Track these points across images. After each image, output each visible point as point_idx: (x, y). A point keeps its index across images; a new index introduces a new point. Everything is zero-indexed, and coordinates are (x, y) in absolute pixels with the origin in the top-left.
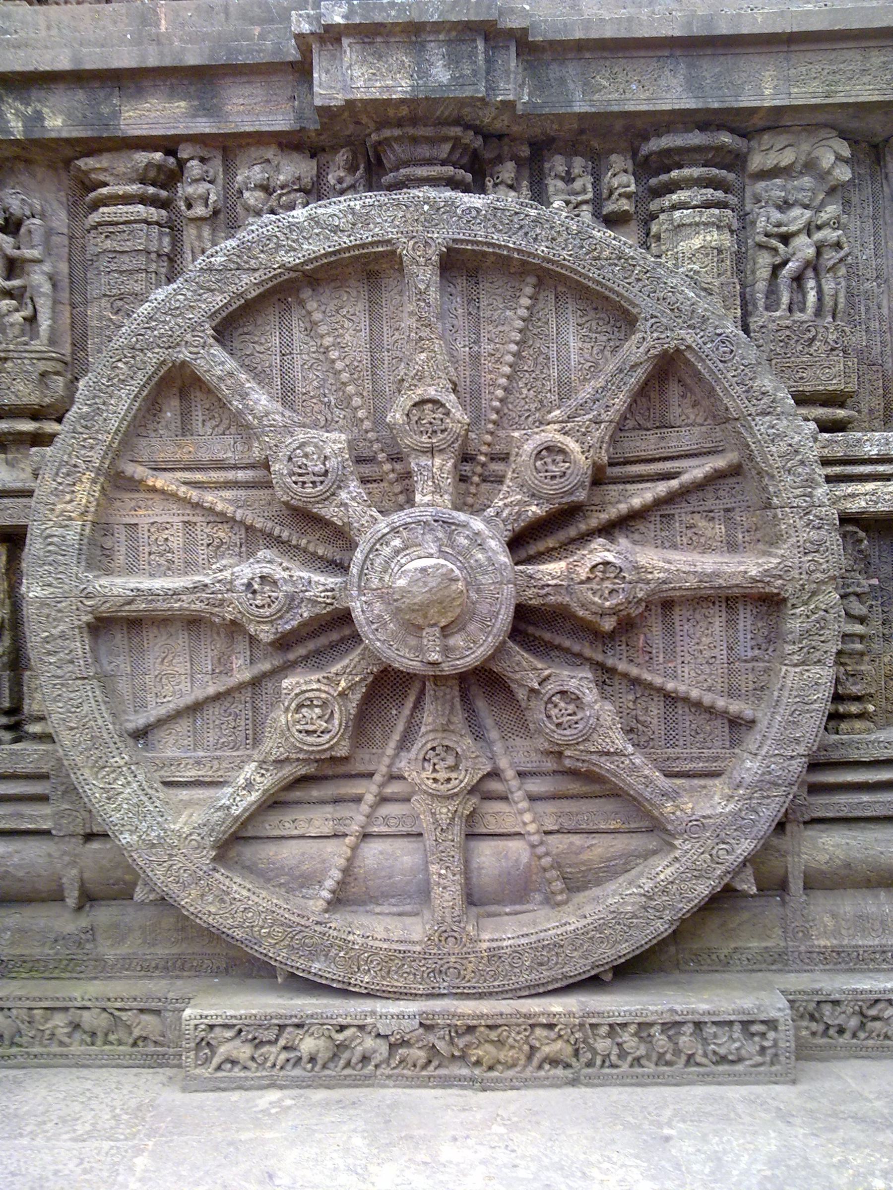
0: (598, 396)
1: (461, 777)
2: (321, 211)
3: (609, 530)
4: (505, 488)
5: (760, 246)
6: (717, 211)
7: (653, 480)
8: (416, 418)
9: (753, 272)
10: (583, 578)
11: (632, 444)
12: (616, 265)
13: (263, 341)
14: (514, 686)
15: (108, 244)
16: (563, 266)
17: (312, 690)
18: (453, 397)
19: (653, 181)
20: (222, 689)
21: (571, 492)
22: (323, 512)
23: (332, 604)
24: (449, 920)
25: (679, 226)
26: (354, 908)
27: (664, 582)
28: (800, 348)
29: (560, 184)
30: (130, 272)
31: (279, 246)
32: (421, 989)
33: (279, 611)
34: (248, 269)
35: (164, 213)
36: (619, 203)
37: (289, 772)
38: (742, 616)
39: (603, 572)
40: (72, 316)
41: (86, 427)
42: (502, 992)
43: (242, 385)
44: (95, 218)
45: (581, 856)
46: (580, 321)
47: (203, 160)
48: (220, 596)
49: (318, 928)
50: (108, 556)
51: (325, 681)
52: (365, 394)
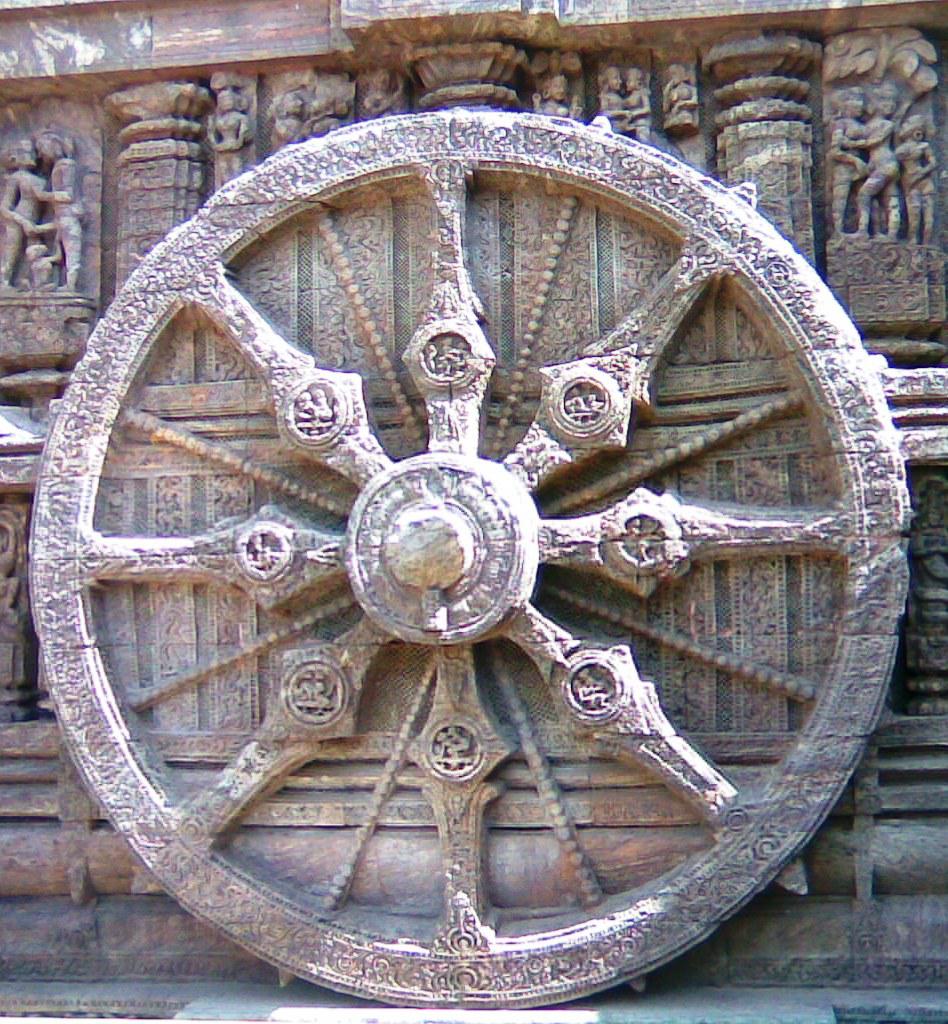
1: (476, 762)
5: (838, 161)
6: (785, 124)
7: (707, 423)
9: (831, 189)
13: (281, 276)
14: (536, 659)
15: (137, 182)
16: (599, 187)
17: (314, 662)
25: (744, 140)
27: (710, 539)
28: (880, 273)
29: (615, 98)
35: (196, 146)
36: (680, 116)
40: (103, 257)
44: (125, 155)
45: (616, 853)
47: (236, 89)
50: (117, 514)
51: (327, 652)
52: (387, 329)
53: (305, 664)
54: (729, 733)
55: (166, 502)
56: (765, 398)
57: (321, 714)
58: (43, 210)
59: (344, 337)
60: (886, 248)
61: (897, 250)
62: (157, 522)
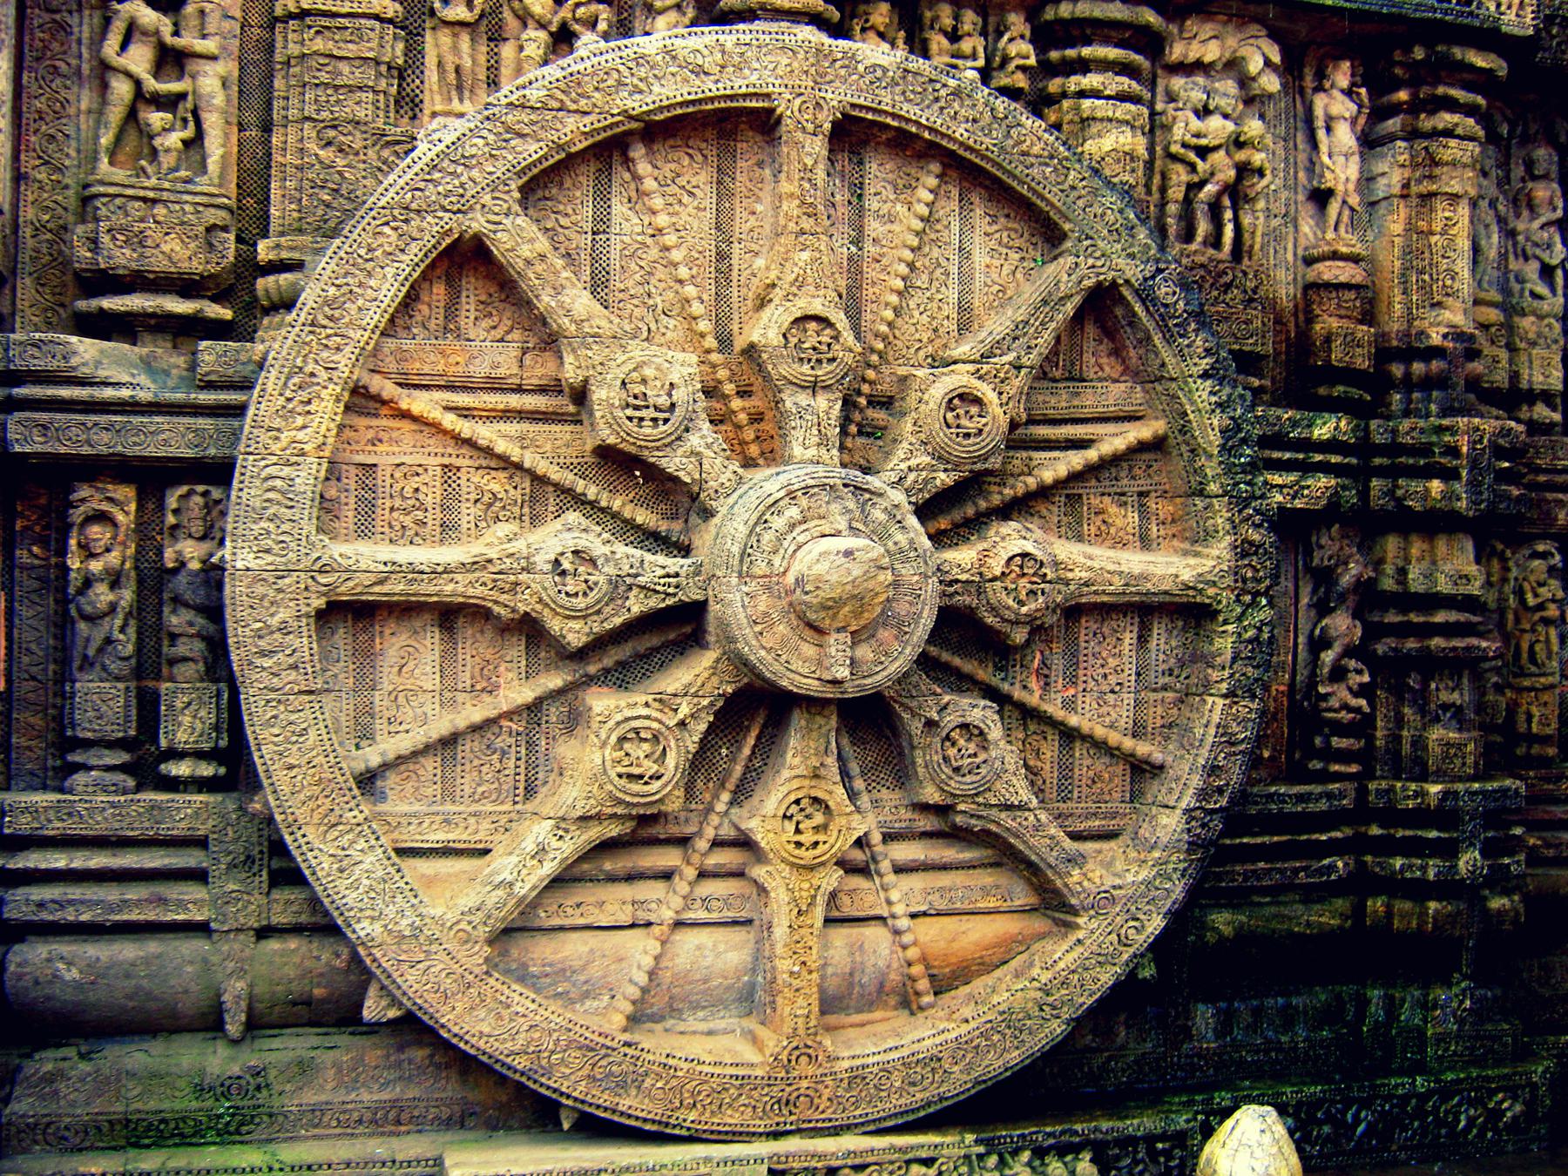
0: (1018, 333)
1: (832, 840)
2: (678, 42)
3: (1006, 512)
4: (905, 445)
6: (1133, 107)
8: (795, 340)
10: (998, 573)
11: (1041, 398)
12: (1047, 165)
13: (570, 212)
15: (319, 44)
16: (983, 157)
18: (842, 315)
19: (1054, 55)
20: (493, 713)
21: (985, 458)
22: (663, 463)
23: (674, 595)
24: (801, 1031)
26: (649, 1025)
29: (945, 42)
30: (351, 89)
31: (620, 83)
32: (761, 1125)
33: (598, 602)
34: (576, 111)
37: (595, 833)
38: (1156, 631)
39: (1021, 567)
40: (240, 144)
41: (331, 318)
42: (862, 1124)
43: (556, 273)
46: (990, 230)
48: (512, 578)
49: (630, 1051)
51: (656, 705)
52: (705, 297)
53: (627, 719)
54: (1069, 804)
55: (404, 498)
56: (1126, 426)
57: (646, 783)
58: (171, 59)
59: (651, 302)
60: (1221, 266)
61: (1232, 269)
62: (391, 527)
